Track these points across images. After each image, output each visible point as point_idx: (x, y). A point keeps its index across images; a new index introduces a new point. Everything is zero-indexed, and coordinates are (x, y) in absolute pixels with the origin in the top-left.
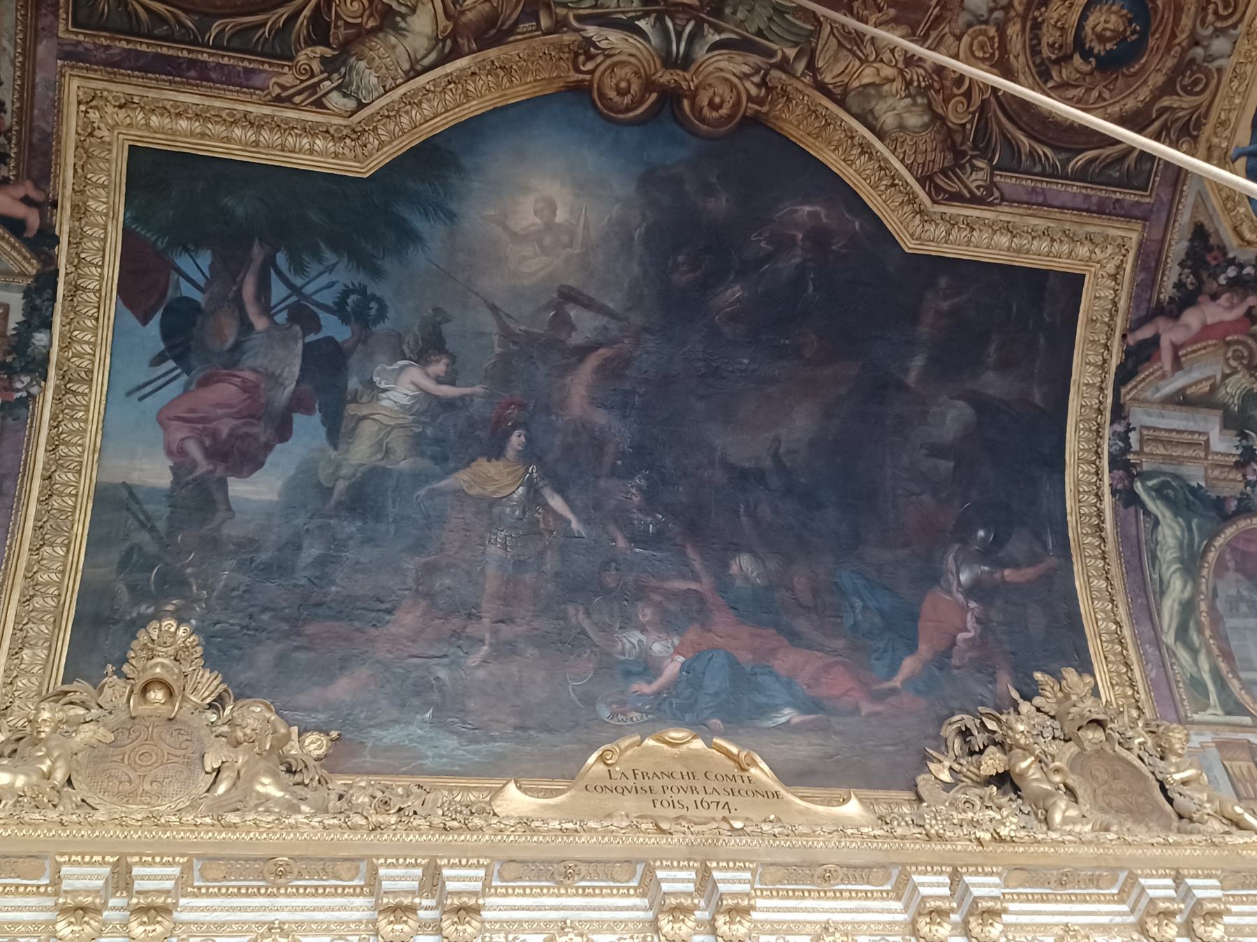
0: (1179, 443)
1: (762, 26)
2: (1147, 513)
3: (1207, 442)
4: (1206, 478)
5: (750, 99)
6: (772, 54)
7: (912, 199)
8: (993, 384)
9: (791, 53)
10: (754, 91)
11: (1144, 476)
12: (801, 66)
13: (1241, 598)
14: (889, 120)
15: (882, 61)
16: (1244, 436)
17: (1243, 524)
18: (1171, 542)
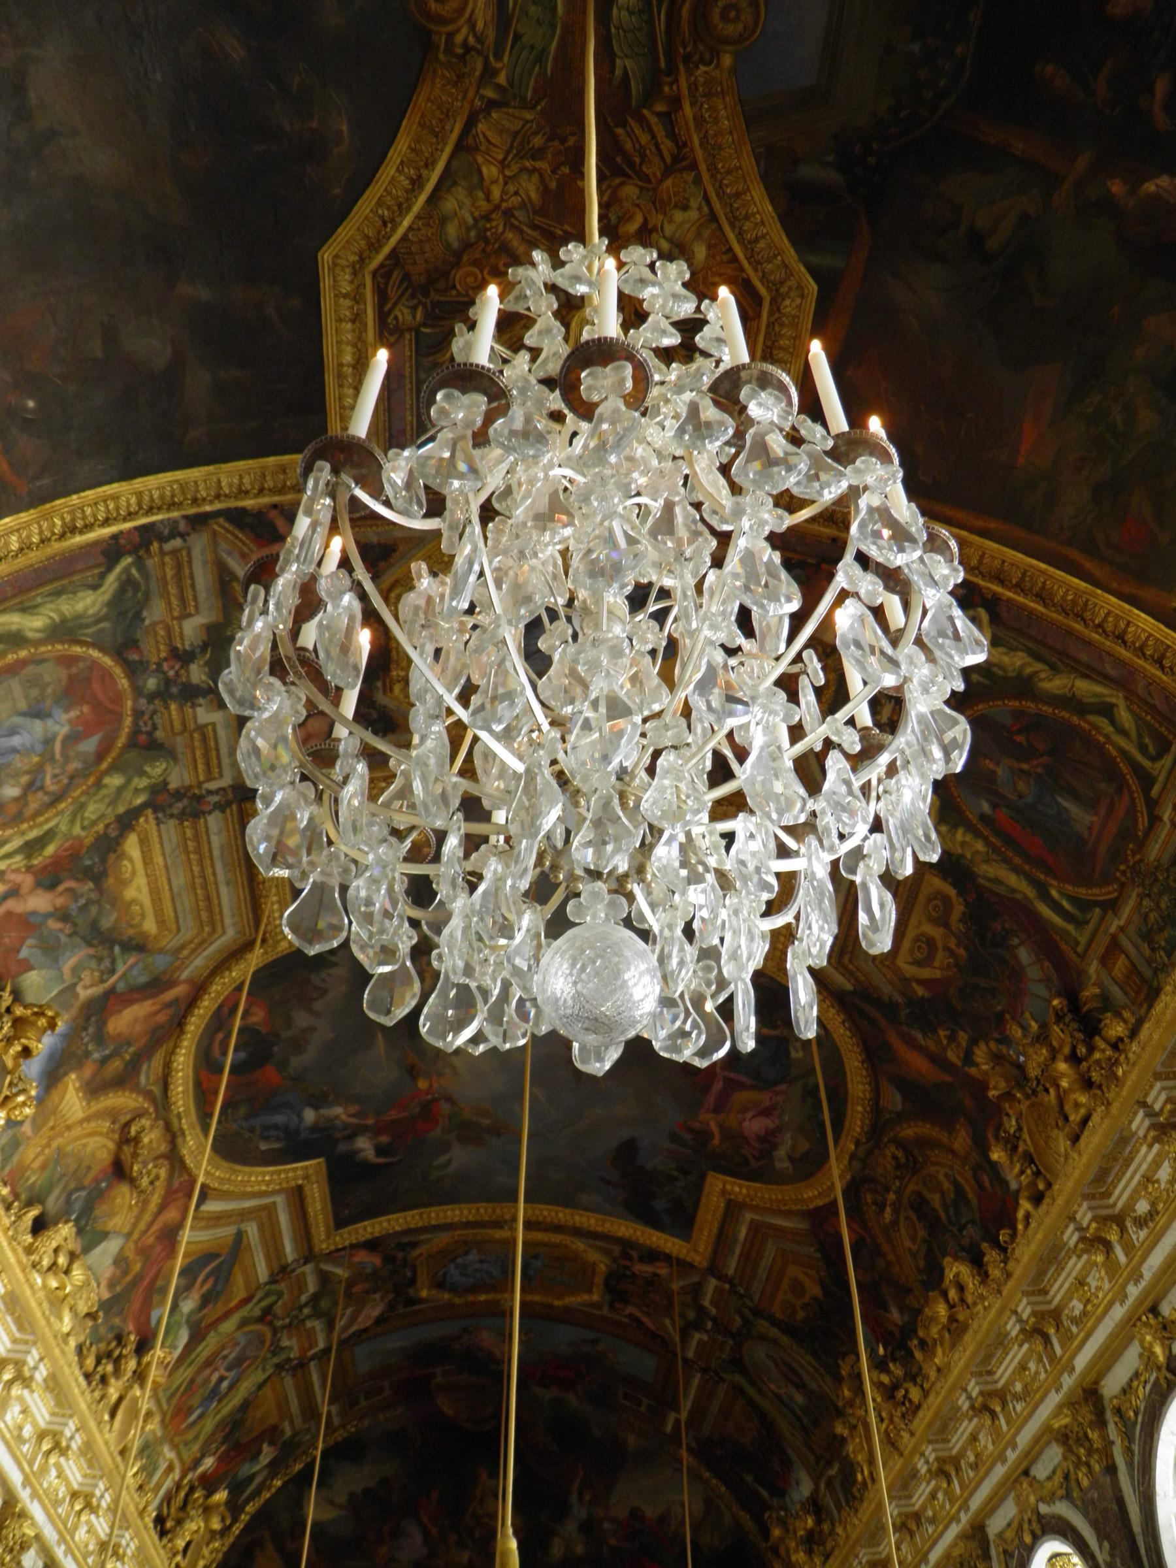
0: (181, 589)
1: (524, 39)
2: (103, 576)
3: (190, 615)
4: (154, 624)
5: (450, 36)
6: (498, 56)
7: (374, 246)
8: (198, 381)
9: (502, 79)
10: (459, 39)
11: (140, 564)
12: (490, 93)
13: (43, 688)
14: (449, 204)
15: (506, 183)
16: (204, 647)
17: (118, 671)
18: (80, 607)
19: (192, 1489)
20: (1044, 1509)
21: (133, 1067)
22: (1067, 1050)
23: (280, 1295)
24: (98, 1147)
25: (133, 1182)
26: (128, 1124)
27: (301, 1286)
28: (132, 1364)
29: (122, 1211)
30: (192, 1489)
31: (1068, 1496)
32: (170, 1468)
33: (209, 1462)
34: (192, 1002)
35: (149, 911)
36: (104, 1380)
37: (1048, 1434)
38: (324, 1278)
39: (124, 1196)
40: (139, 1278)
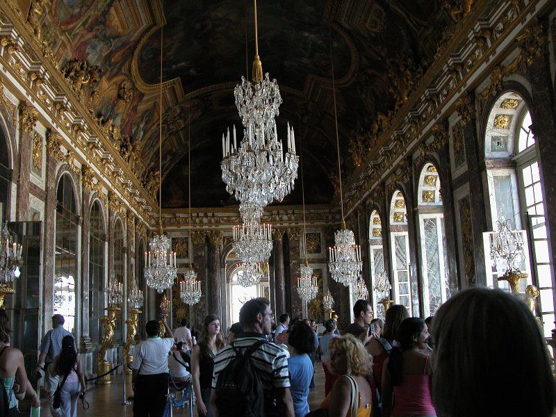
19: (149, 172)
20: (397, 182)
21: (120, 69)
22: (410, 67)
23: (169, 115)
24: (113, 93)
25: (123, 98)
26: (121, 84)
27: (175, 111)
28: (131, 148)
29: (122, 107)
30: (149, 172)
31: (402, 181)
32: (142, 168)
33: (152, 164)
34: (135, 47)
35: (120, 26)
36: (124, 153)
37: (398, 166)
38: (182, 109)
39: (122, 102)
40: (128, 122)
